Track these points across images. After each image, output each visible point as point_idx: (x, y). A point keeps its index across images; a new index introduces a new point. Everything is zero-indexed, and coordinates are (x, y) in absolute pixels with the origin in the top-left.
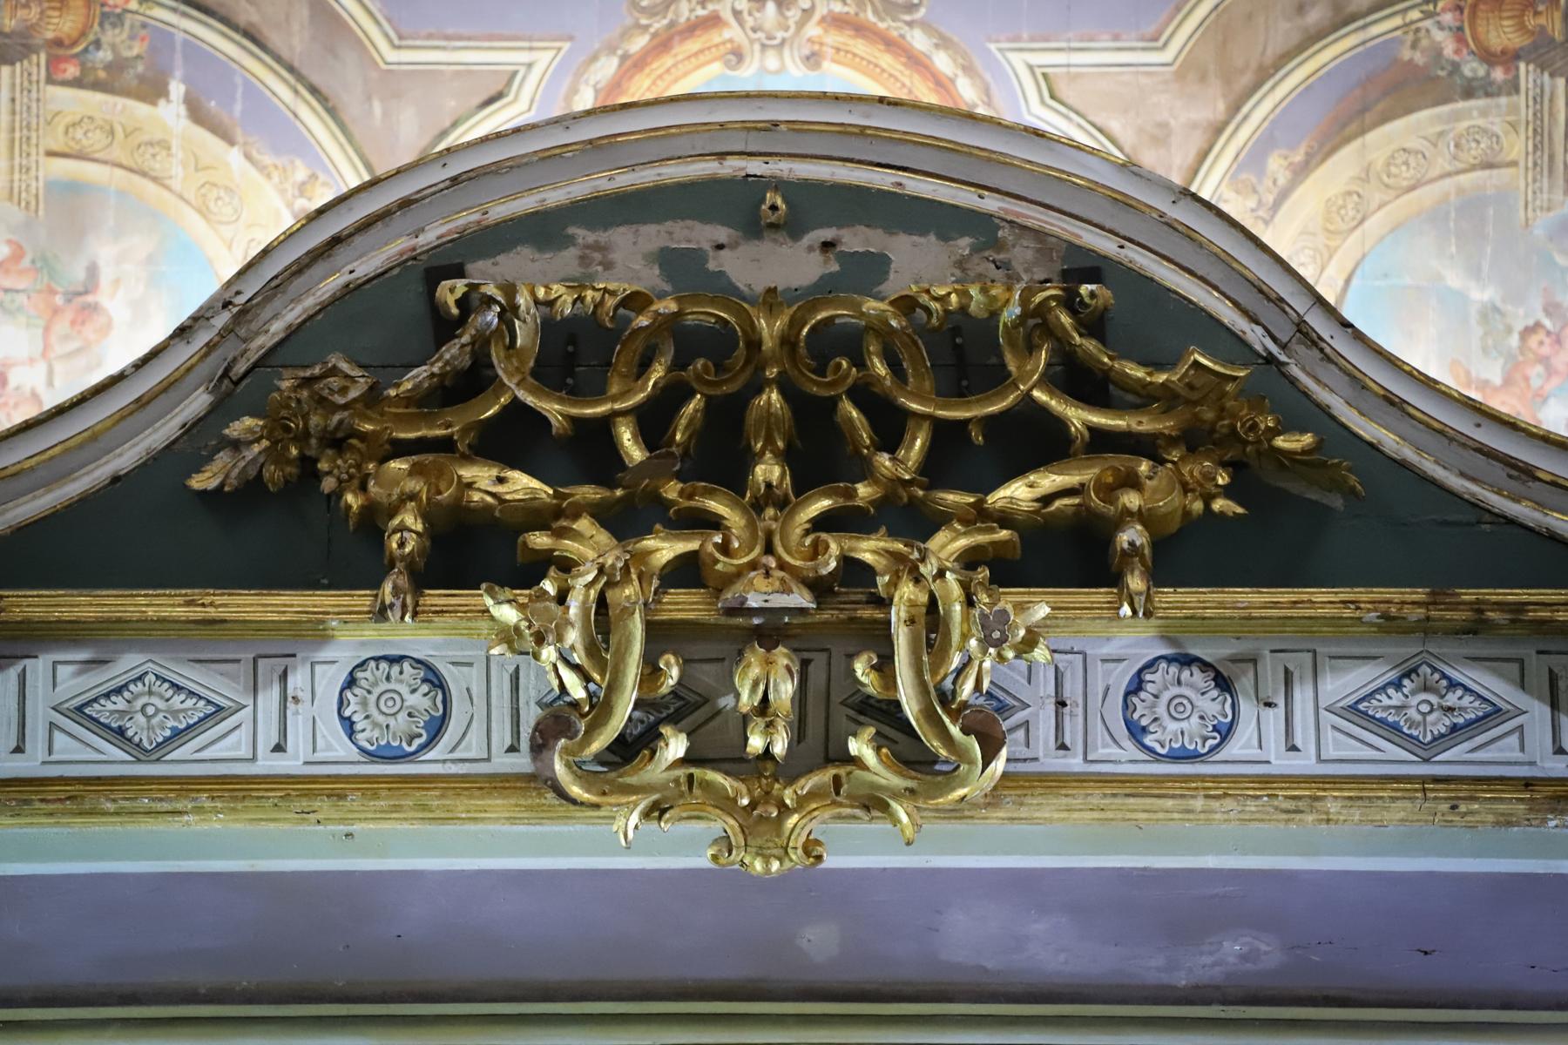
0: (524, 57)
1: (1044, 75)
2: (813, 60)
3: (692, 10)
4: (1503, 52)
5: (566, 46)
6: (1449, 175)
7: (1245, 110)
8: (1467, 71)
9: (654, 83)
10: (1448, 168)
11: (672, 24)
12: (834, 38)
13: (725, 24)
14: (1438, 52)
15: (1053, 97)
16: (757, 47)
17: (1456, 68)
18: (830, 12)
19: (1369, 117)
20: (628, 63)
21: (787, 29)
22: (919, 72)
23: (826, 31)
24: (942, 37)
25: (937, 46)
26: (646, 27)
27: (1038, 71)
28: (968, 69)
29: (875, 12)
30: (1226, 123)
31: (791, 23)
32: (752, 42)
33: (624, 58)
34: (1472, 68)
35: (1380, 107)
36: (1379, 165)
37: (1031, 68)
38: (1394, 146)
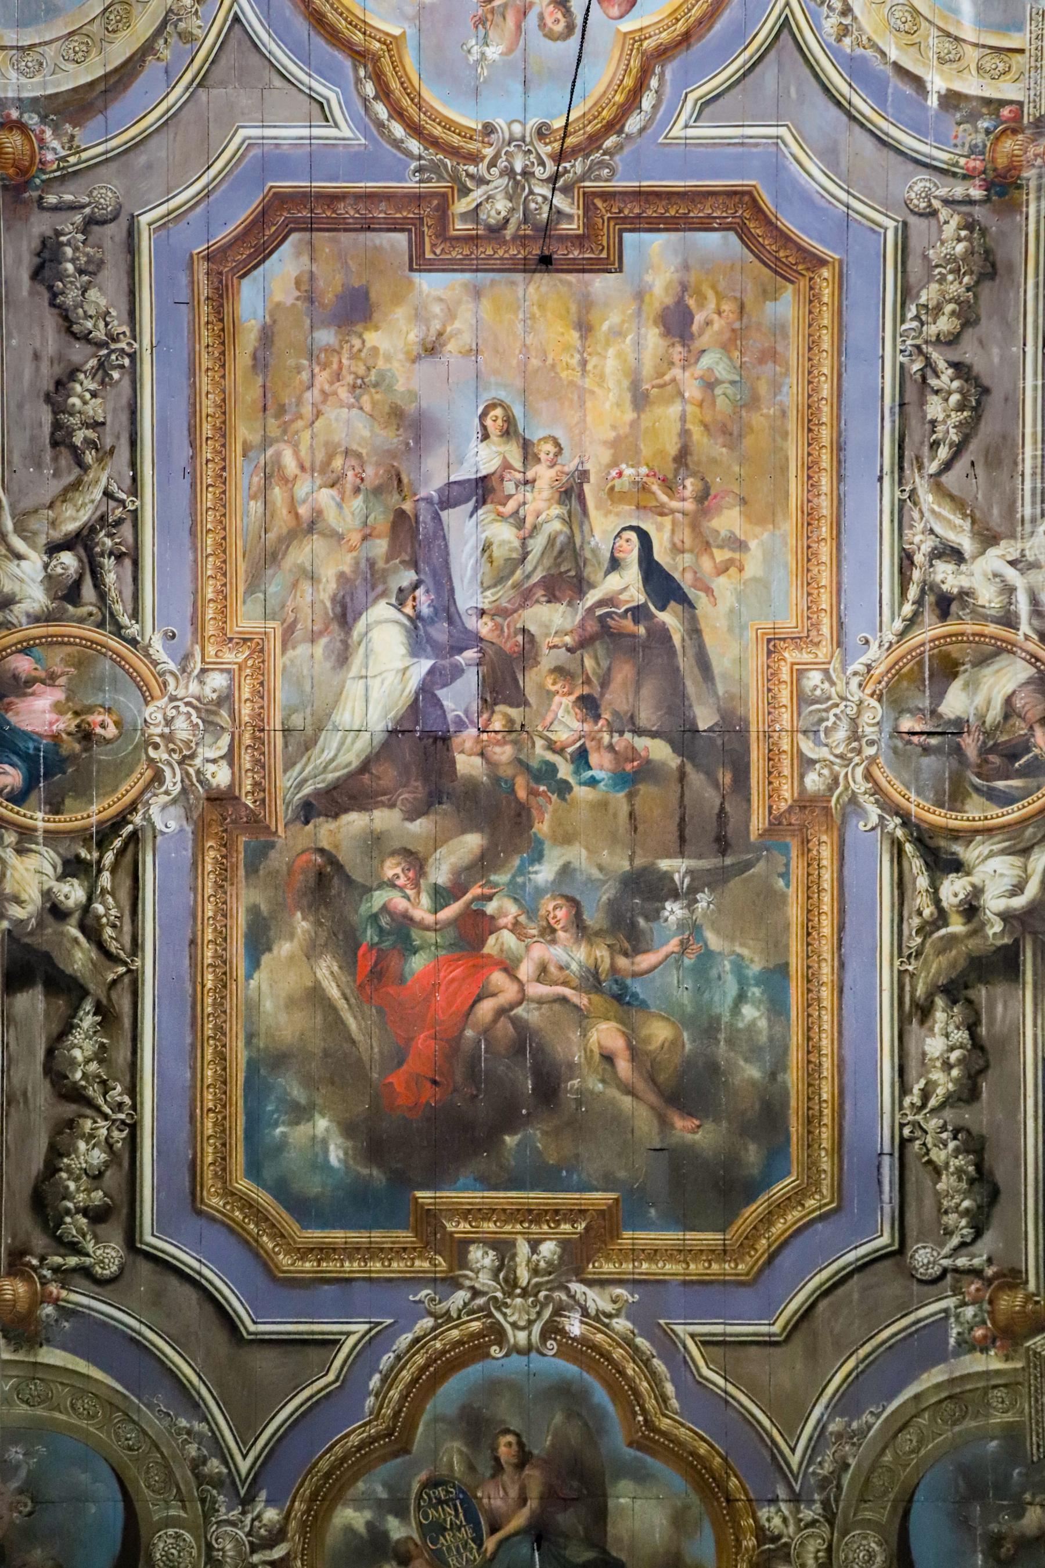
0: (691, 132)
1: (327, 120)
2: (489, 129)
3: (573, 166)
4: (11, 129)
5: (661, 140)
6: (46, 43)
7: (187, 94)
8: (36, 118)
9: (600, 113)
10: (46, 48)
11: (587, 156)
12: (473, 146)
13: (551, 156)
14: (56, 129)
15: (321, 104)
16: (528, 139)
17: (44, 119)
18: (477, 166)
19: (102, 87)
20: (618, 127)
21: (506, 153)
22: (414, 123)
23: (479, 151)
24: (398, 148)
25: (402, 141)
26: (604, 154)
27: (331, 123)
28: (380, 125)
29: (445, 165)
30: (199, 85)
31: (504, 158)
32: (531, 143)
33: (620, 132)
34: (32, 120)
35: (95, 94)
36: (94, 52)
37: (336, 126)
38: (83, 66)
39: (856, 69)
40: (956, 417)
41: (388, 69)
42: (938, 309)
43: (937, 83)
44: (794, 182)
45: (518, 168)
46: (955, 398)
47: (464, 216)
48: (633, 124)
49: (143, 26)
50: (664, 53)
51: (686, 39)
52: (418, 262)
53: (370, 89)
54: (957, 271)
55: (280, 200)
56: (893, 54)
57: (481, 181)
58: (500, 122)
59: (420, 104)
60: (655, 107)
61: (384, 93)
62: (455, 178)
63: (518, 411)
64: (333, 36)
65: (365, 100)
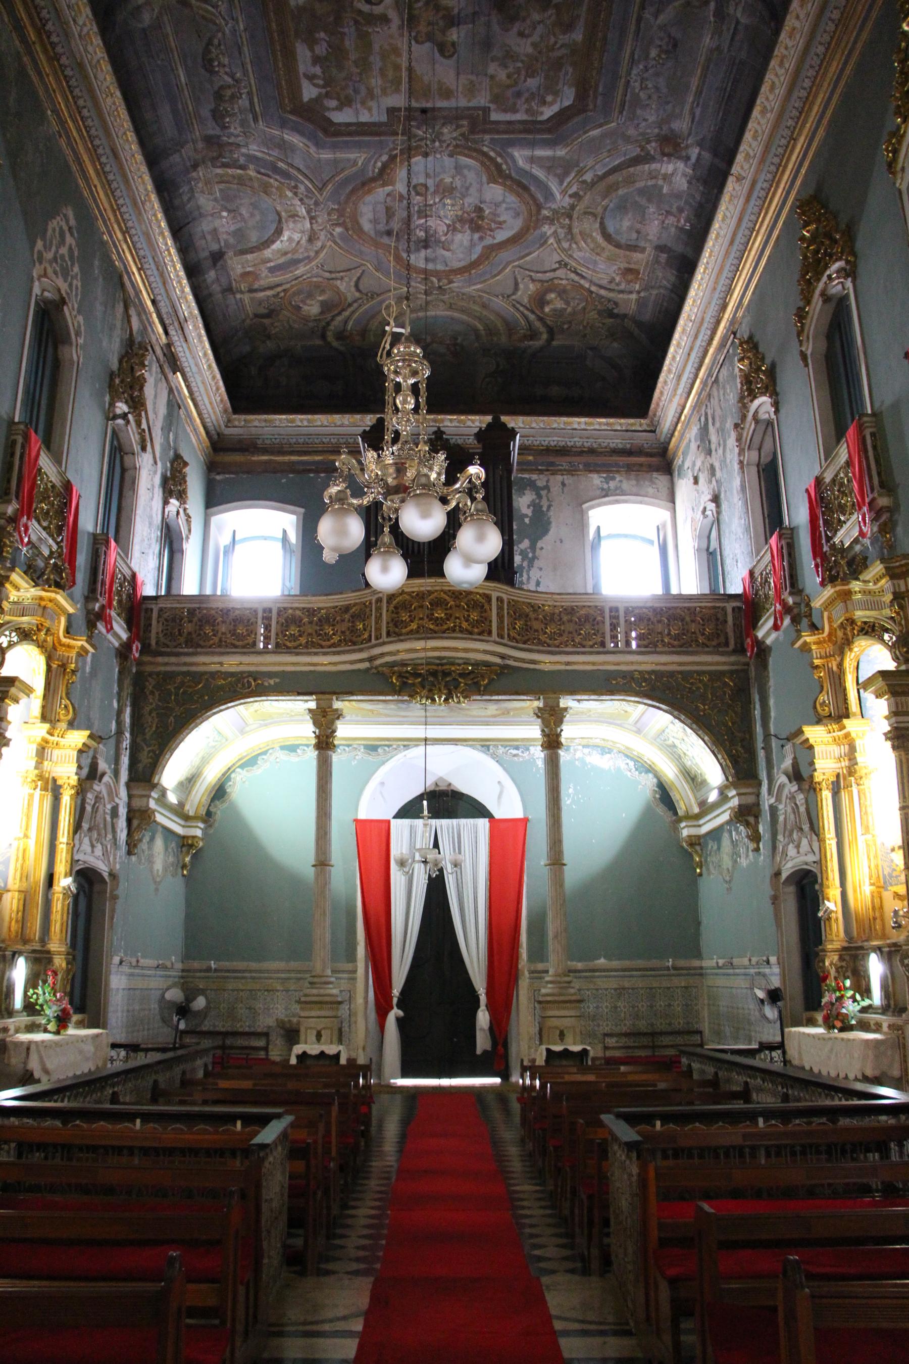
2: (451, 156)
28: (501, 156)
39: (286, 175)
40: (213, 55)
41: (495, 173)
42: (233, 97)
43: (252, 173)
44: (309, 139)
45: (437, 144)
46: (216, 63)
47: (462, 126)
48: (385, 158)
49: (602, 186)
50: (373, 180)
51: (364, 184)
52: (486, 111)
53: (504, 167)
54: (227, 111)
55: (549, 131)
56: (272, 181)
57: (454, 139)
58: (446, 158)
59: (483, 164)
60: (375, 162)
61: (498, 166)
62: (467, 140)
63: (437, 55)
64: (520, 184)
65: (506, 163)
